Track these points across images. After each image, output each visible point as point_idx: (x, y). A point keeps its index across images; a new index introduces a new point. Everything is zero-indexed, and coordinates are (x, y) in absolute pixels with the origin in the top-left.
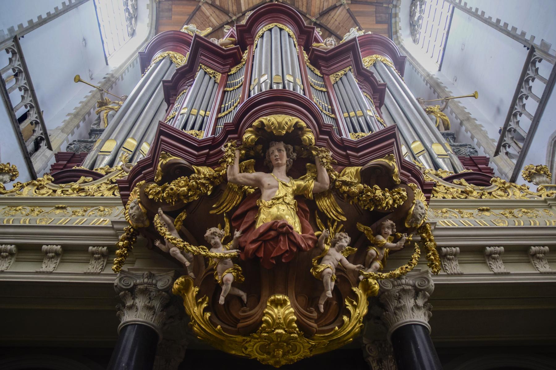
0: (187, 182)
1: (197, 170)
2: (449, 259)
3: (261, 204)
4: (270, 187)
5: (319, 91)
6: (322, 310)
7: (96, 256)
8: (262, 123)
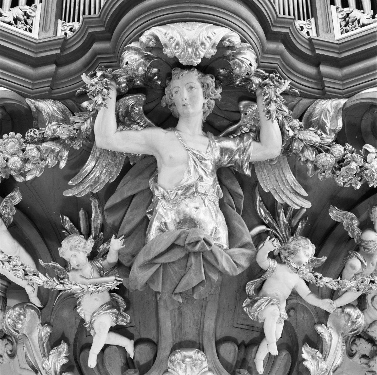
0: (21, 145)
1: (37, 108)
3: (156, 193)
8: (156, 38)
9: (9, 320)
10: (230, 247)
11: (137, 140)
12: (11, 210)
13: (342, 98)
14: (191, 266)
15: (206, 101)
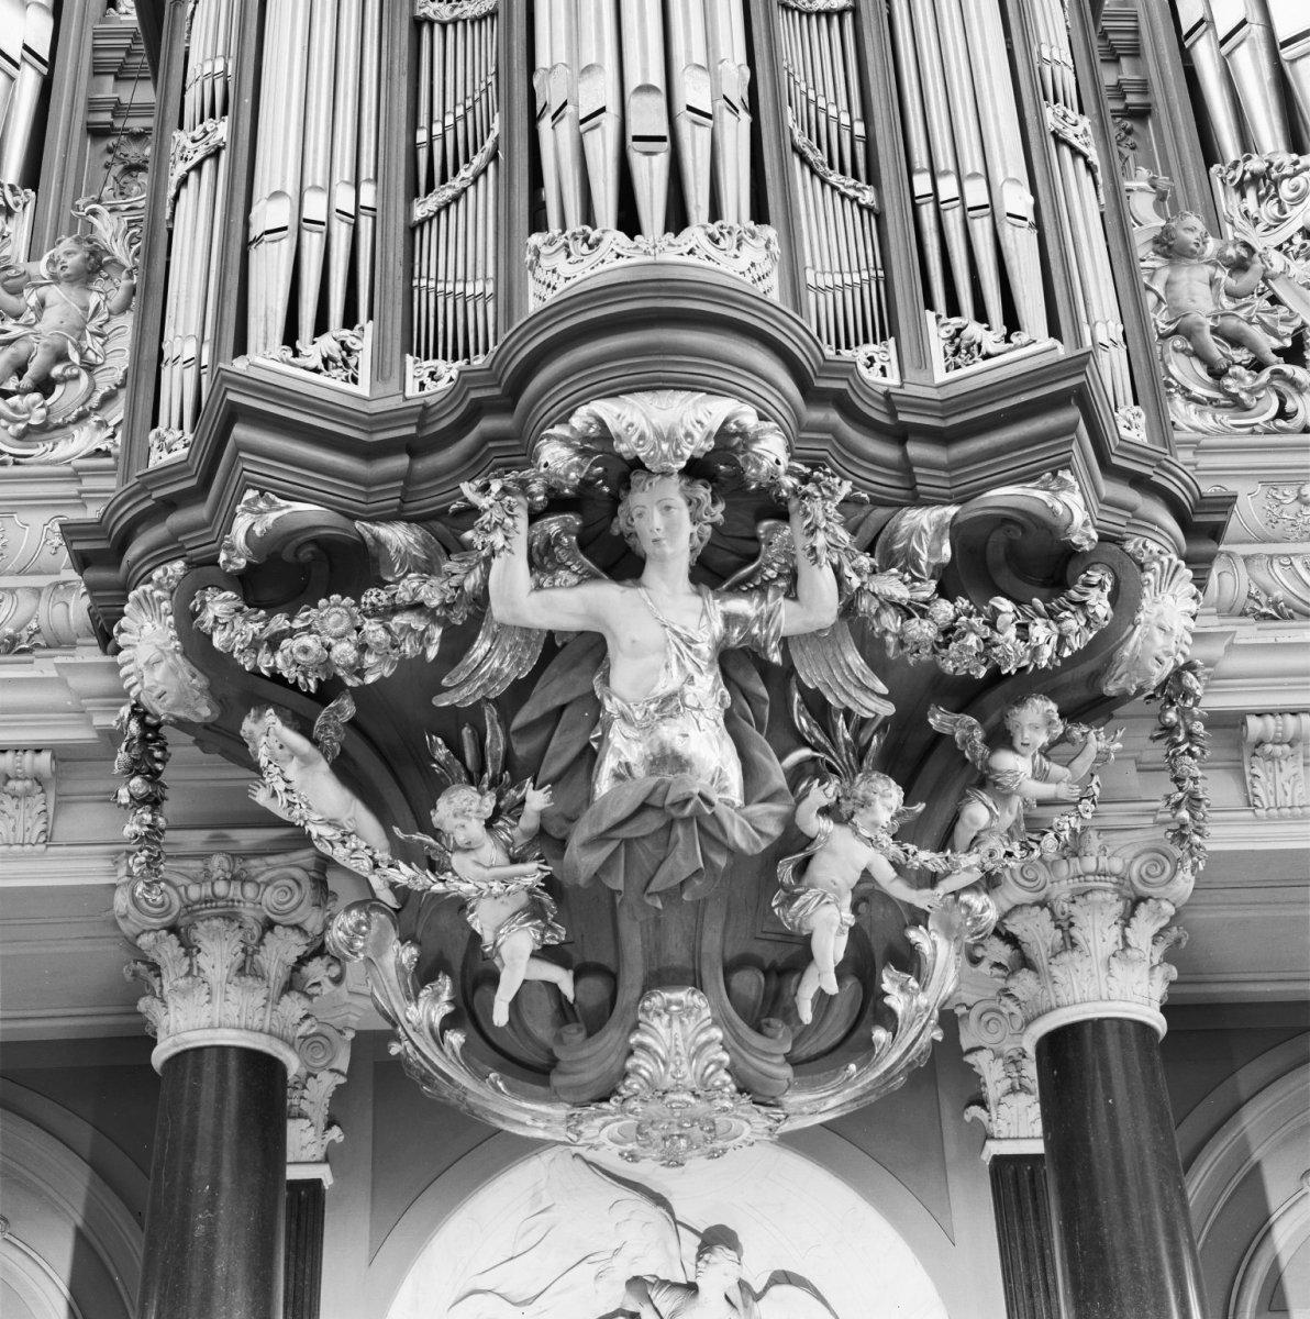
0: (353, 619)
1: (376, 539)
2: (1271, 758)
3: (608, 706)
4: (637, 651)
5: (819, 13)
6: (807, 1015)
7: (18, 786)
9: (341, 934)
10: (747, 802)
11: (569, 604)
12: (337, 732)
13: (949, 504)
14: (677, 842)
15: (695, 529)
